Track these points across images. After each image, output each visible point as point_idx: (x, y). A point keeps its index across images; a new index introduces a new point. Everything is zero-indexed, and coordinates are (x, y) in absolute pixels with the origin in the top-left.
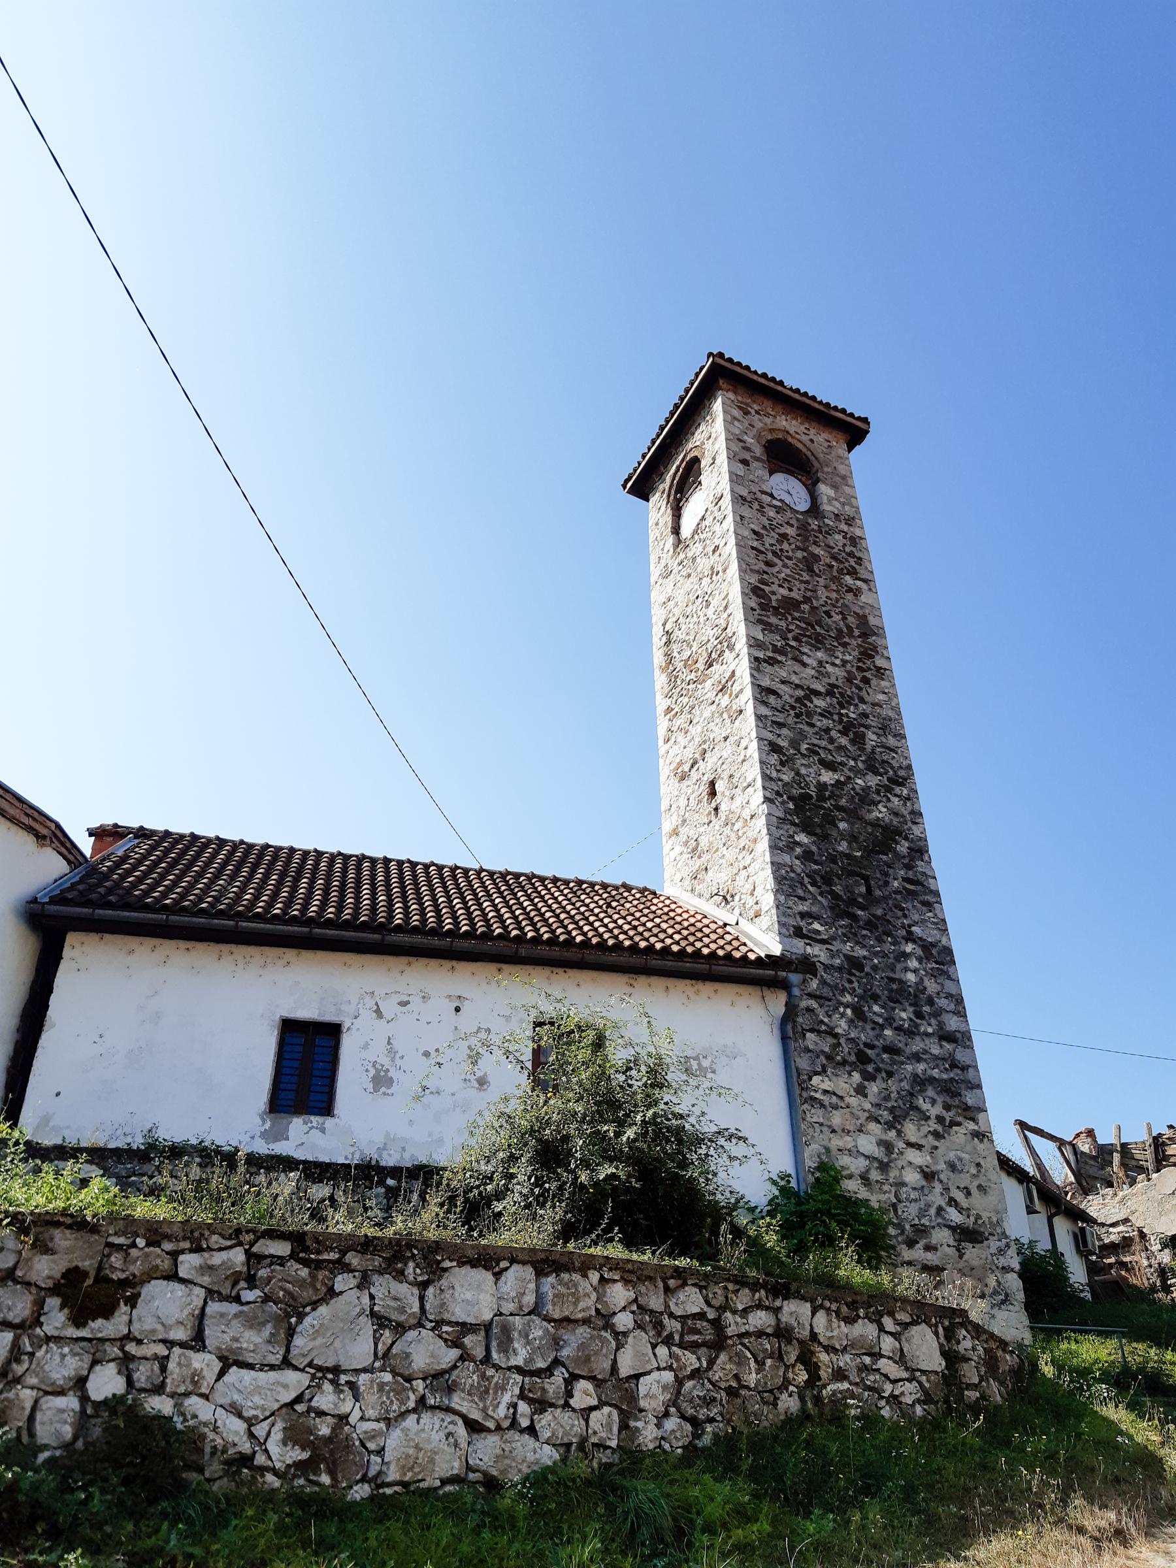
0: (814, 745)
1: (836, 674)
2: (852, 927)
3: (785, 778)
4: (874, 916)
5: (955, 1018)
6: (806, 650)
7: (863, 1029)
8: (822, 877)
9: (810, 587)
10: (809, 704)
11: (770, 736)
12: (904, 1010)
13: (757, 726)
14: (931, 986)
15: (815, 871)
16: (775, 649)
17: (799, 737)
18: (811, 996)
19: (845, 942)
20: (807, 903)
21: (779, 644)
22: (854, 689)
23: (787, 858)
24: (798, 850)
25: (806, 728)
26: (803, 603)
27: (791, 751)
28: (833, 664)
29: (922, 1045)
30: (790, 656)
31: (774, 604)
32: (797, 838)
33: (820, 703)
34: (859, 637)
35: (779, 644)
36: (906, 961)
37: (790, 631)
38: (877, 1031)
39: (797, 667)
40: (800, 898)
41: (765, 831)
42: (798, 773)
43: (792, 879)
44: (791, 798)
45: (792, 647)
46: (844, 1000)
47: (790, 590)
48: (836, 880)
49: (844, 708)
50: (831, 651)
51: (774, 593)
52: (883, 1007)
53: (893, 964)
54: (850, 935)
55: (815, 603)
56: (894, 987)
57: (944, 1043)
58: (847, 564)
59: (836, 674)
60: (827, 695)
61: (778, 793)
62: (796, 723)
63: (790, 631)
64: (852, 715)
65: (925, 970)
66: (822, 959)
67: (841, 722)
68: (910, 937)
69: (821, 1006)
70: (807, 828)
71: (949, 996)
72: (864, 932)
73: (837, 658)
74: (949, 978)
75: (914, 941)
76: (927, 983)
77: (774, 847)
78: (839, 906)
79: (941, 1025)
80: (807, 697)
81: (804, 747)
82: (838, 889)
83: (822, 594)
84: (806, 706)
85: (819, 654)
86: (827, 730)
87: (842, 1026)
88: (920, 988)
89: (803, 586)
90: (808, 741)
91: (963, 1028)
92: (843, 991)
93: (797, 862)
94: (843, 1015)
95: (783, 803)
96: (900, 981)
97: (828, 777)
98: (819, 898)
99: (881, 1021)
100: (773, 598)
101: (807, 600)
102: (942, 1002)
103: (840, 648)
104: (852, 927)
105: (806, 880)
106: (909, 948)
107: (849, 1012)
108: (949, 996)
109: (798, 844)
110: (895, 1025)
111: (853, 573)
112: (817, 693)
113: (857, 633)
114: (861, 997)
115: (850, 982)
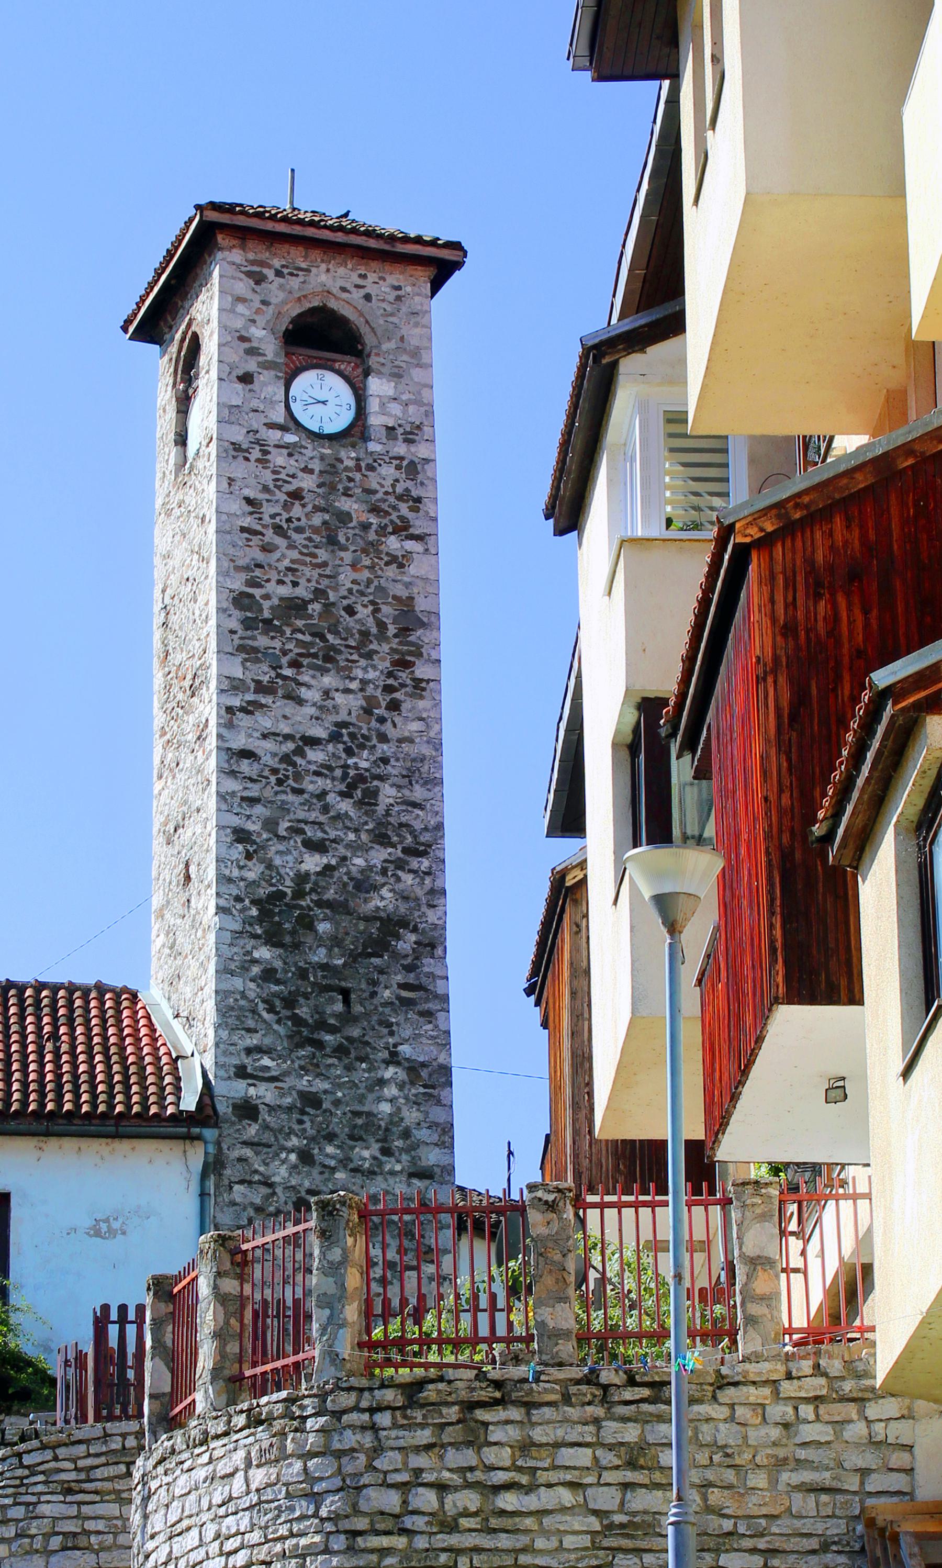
0: (299, 821)
1: (348, 705)
2: (314, 1057)
3: (251, 875)
4: (348, 1039)
5: (437, 1150)
6: (305, 678)
7: (309, 1174)
8: (283, 999)
9: (328, 572)
10: (299, 760)
11: (236, 821)
12: (367, 1148)
13: (218, 810)
14: (411, 1116)
15: (275, 995)
16: (260, 688)
17: (278, 814)
18: (245, 1143)
19: (302, 1076)
20: (258, 1035)
21: (266, 679)
22: (374, 724)
23: (238, 983)
24: (256, 970)
25: (291, 797)
26: (311, 601)
27: (265, 836)
28: (347, 691)
29: (384, 1186)
30: (280, 692)
31: (267, 614)
32: (256, 955)
33: (316, 756)
34: (395, 636)
35: (266, 679)
36: (381, 1088)
37: (285, 653)
38: (326, 1175)
39: (289, 708)
40: (249, 1030)
41: (214, 950)
42: (270, 866)
43: (241, 1008)
44: (253, 902)
45: (285, 678)
46: (289, 1144)
47: (295, 584)
48: (302, 1000)
49: (349, 752)
50: (346, 673)
51: (267, 597)
52: (338, 1147)
53: (363, 1095)
54: (312, 1067)
55: (332, 596)
56: (360, 1121)
57: (415, 1181)
58: (394, 516)
59: (348, 705)
60: (329, 741)
61: (238, 899)
62: (276, 793)
63: (285, 653)
64: (364, 764)
65: (406, 1098)
66: (267, 1101)
67: (345, 775)
68: (394, 1059)
69: (257, 1153)
70: (272, 939)
71: (433, 1125)
72: (330, 1061)
73: (352, 679)
74: (439, 1102)
75: (398, 1064)
76: (405, 1113)
77: (223, 971)
78: (300, 1033)
79: (414, 1161)
80: (299, 752)
81: (284, 825)
82: (303, 1011)
83: (346, 578)
84: (294, 765)
85: (328, 680)
86: (323, 794)
87: (280, 1174)
88: (396, 1118)
89: (315, 573)
90: (292, 816)
91: (445, 1160)
92: (291, 1132)
93: (252, 985)
94: (283, 1162)
95: (242, 911)
96: (369, 1114)
97: (313, 863)
98: (276, 1027)
99: (333, 1163)
100: (266, 604)
101: (319, 593)
102: (422, 1134)
103: (363, 662)
104: (314, 1057)
105: (261, 1006)
106: (389, 1072)
107: (293, 1157)
108: (433, 1125)
109: (255, 961)
110: (351, 1166)
111: (402, 529)
112: (313, 742)
113: (392, 630)
114: (313, 1139)
115: (300, 1122)
